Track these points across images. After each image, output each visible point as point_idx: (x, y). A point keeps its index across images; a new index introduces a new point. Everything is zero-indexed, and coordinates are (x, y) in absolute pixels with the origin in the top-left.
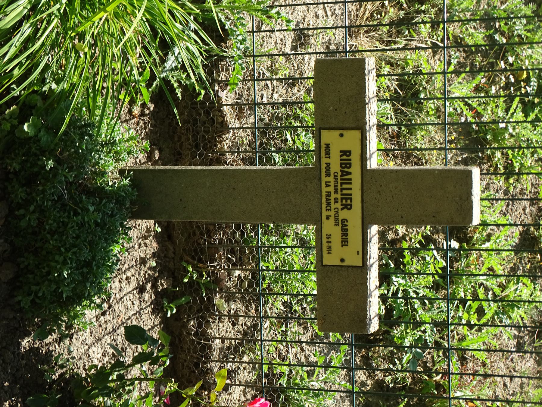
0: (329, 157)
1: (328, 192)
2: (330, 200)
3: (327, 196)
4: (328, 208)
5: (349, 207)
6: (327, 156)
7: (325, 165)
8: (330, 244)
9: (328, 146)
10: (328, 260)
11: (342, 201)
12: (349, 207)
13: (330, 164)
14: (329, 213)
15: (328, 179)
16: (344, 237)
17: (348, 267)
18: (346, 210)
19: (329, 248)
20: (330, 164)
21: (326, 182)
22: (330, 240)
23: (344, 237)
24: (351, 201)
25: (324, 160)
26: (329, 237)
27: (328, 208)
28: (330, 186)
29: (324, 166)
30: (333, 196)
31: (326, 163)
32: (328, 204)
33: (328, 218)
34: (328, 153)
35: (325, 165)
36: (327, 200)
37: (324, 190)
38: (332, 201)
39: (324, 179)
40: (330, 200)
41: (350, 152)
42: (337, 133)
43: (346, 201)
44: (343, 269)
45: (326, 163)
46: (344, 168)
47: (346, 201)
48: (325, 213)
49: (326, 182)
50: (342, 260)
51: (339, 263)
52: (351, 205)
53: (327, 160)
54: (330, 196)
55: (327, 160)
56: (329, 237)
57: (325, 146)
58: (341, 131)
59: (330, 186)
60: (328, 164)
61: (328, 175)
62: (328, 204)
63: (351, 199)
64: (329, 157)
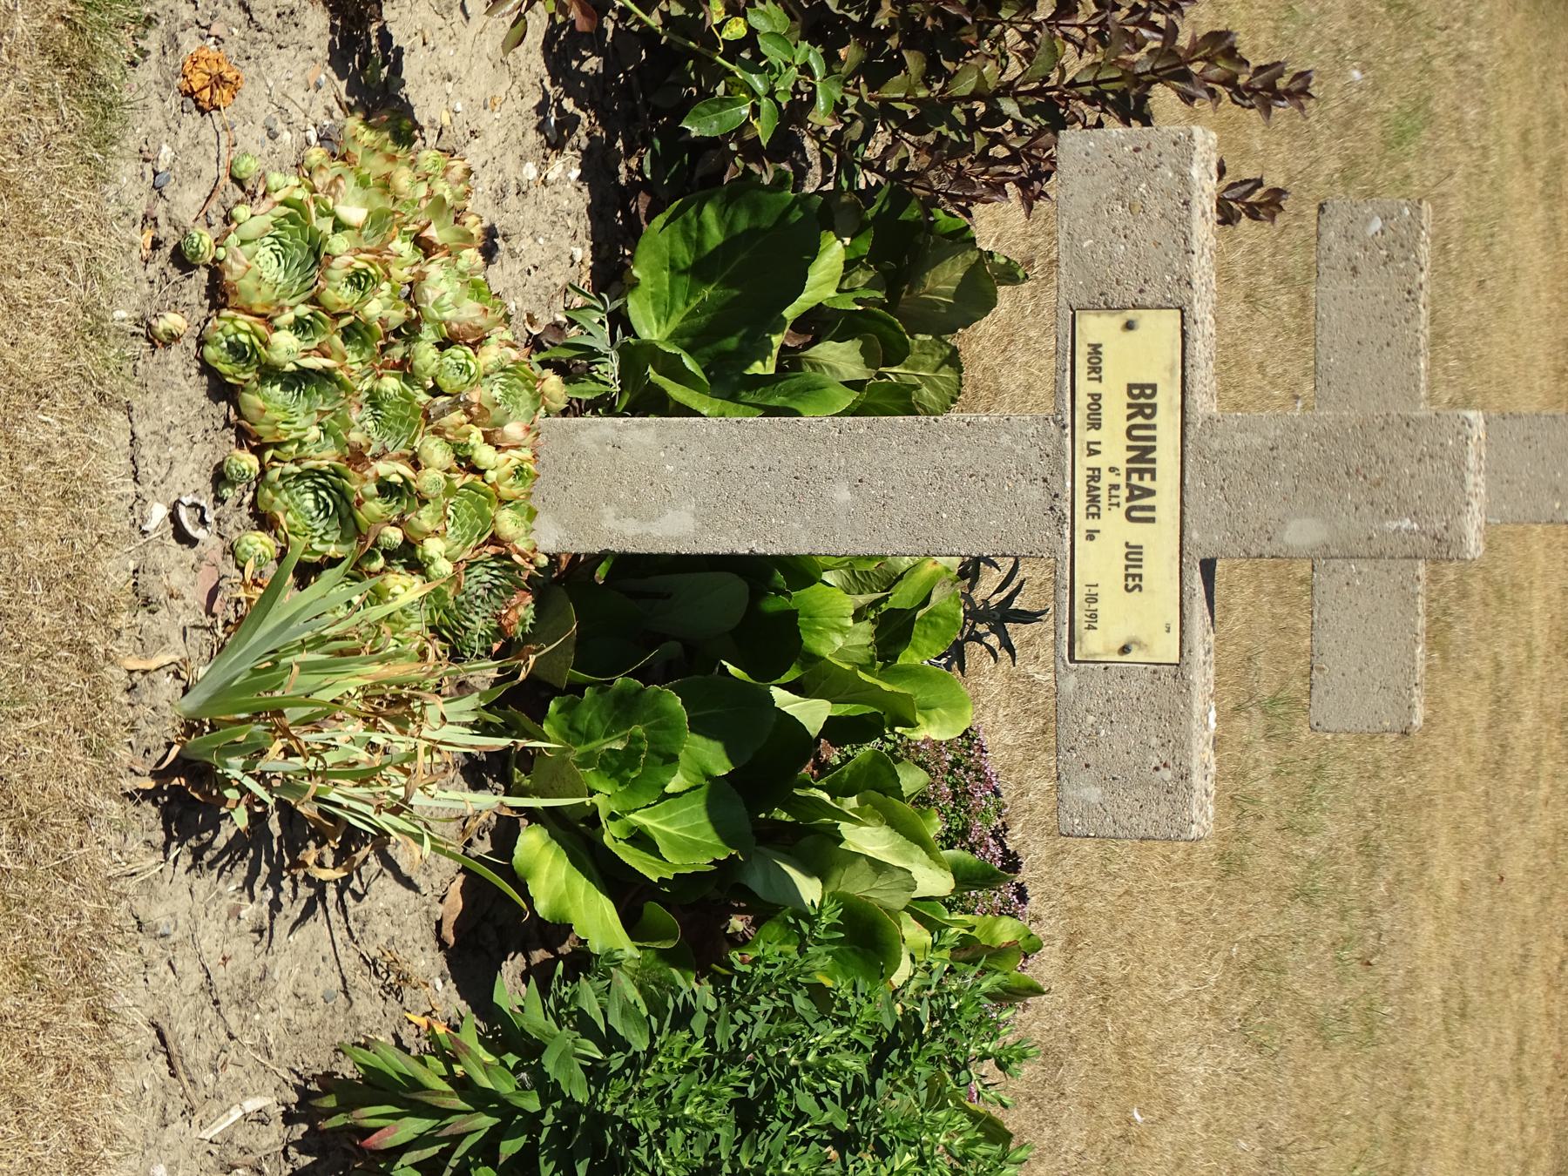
0: (1100, 379)
3: (1092, 478)
6: (1094, 375)
7: (1090, 400)
8: (1093, 606)
9: (1096, 349)
14: (1093, 524)
15: (1093, 435)
19: (1093, 616)
25: (1085, 386)
28: (1098, 452)
29: (1083, 401)
32: (1094, 500)
33: (1091, 536)
34: (1095, 368)
35: (1090, 400)
36: (1091, 489)
37: (1084, 462)
38: (1104, 494)
39: (1085, 435)
41: (1154, 387)
42: (1117, 321)
46: (1137, 397)
48: (1083, 524)
53: (1095, 387)
55: (1095, 387)
58: (1130, 314)
59: (1098, 452)
60: (1096, 398)
61: (1096, 425)
62: (1094, 500)
64: (1100, 379)
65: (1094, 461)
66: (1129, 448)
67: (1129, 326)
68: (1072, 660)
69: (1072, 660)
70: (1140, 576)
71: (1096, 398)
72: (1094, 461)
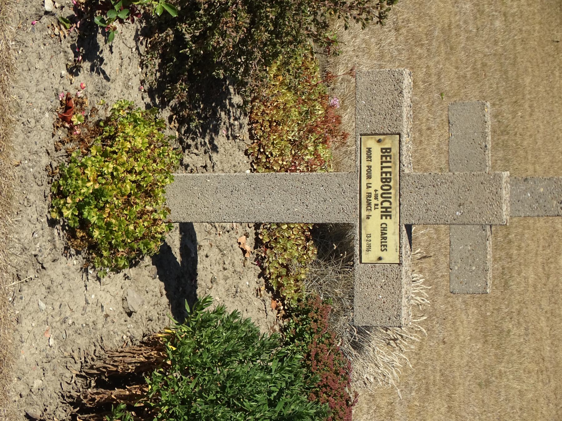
0: (371, 161)
4: (369, 208)
7: (367, 168)
8: (369, 243)
9: (369, 150)
19: (369, 246)
21: (367, 184)
26: (369, 236)
27: (369, 208)
28: (370, 187)
31: (368, 166)
32: (369, 204)
33: (368, 217)
34: (369, 157)
35: (367, 168)
45: (368, 166)
48: (364, 213)
50: (380, 259)
54: (370, 197)
58: (382, 137)
59: (370, 187)
60: (369, 167)
61: (369, 177)
62: (369, 204)
68: (361, 262)
69: (361, 262)
70: (386, 246)
71: (369, 167)
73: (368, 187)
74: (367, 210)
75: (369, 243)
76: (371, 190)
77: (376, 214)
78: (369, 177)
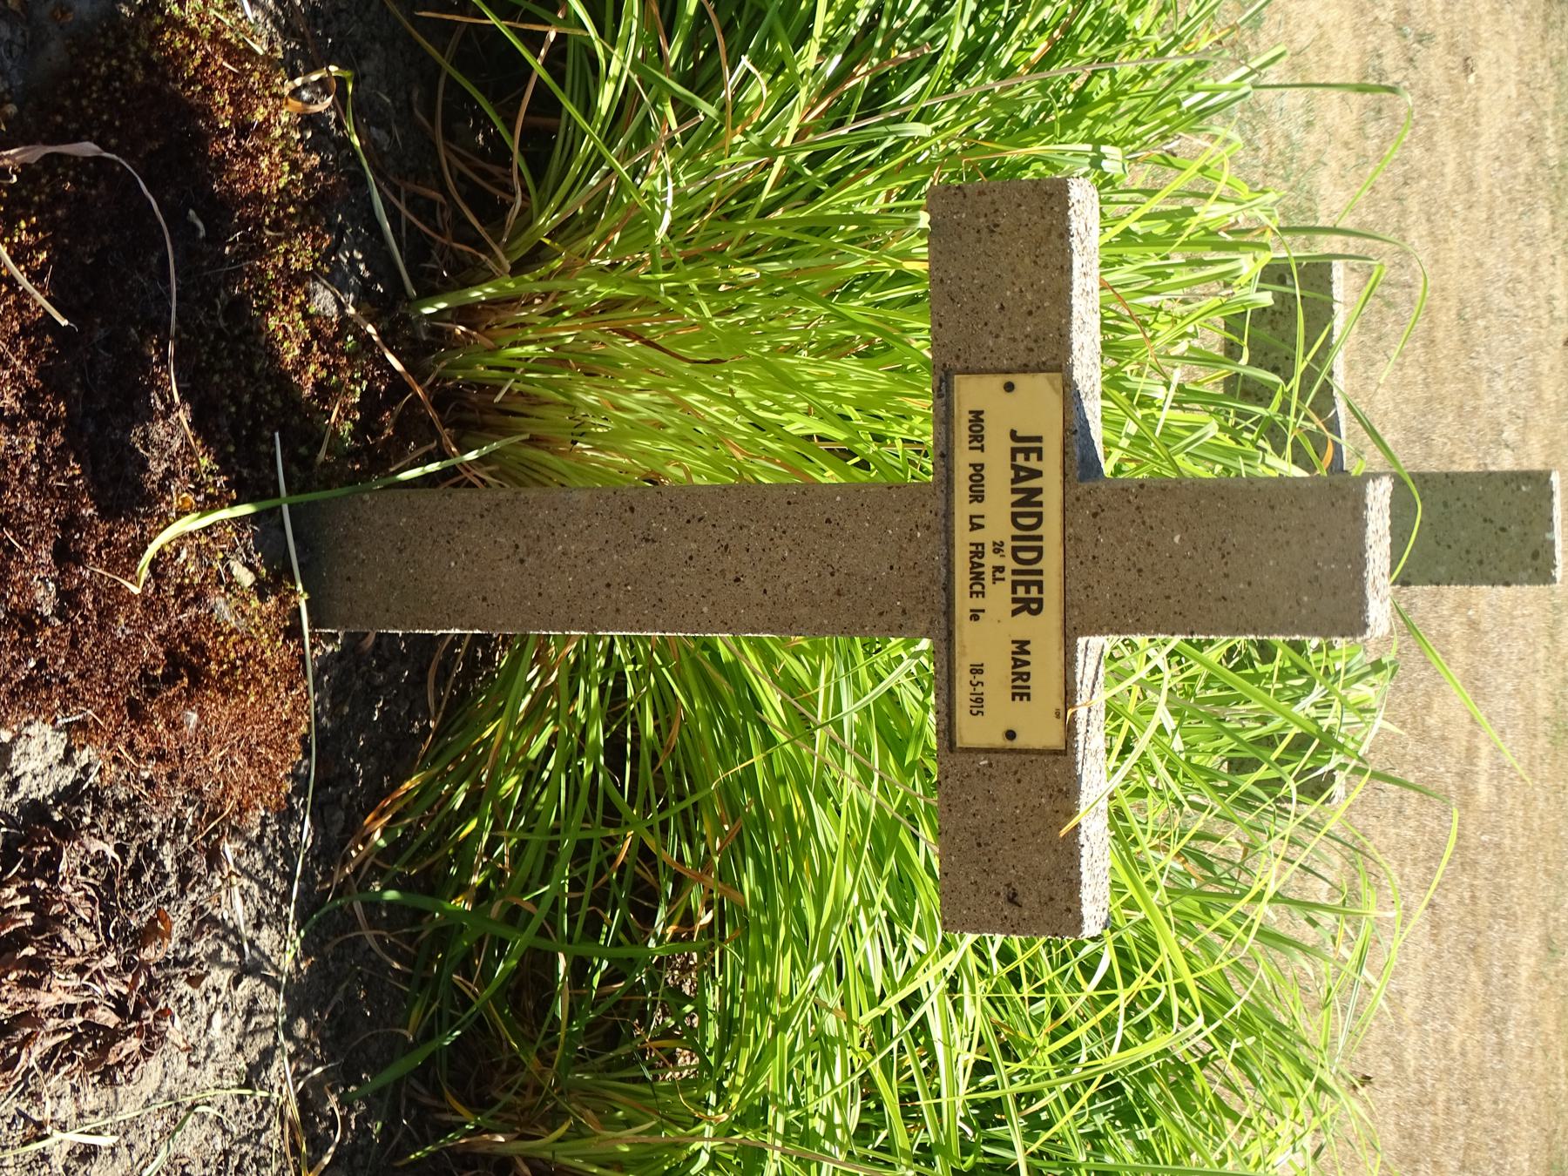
1: (977, 545)
2: (982, 565)
4: (977, 588)
5: (1034, 606)
6: (975, 444)
7: (971, 471)
8: (979, 689)
9: (977, 416)
10: (971, 732)
11: (1014, 591)
12: (1034, 606)
13: (982, 466)
14: (977, 603)
15: (976, 508)
16: (1019, 683)
17: (1027, 751)
18: (1025, 614)
19: (978, 700)
20: (982, 466)
21: (972, 517)
22: (979, 678)
23: (1019, 683)
24: (1040, 591)
26: (977, 670)
27: (977, 588)
28: (981, 527)
30: (990, 560)
31: (973, 465)
32: (977, 578)
33: (975, 616)
34: (977, 437)
36: (974, 565)
37: (963, 538)
39: (963, 508)
40: (982, 565)
43: (1028, 591)
44: (1011, 755)
45: (973, 465)
47: (1028, 591)
48: (963, 603)
49: (972, 517)
50: (1011, 735)
51: (999, 741)
52: (1040, 601)
53: (976, 457)
55: (976, 457)
56: (977, 670)
57: (971, 417)
59: (981, 527)
60: (978, 468)
61: (977, 496)
62: (977, 578)
63: (1040, 585)
65: (977, 536)
66: (1014, 491)
67: (1009, 387)
71: (978, 468)
72: (977, 536)
73: (975, 527)
74: (971, 594)
75: (979, 689)
76: (986, 537)
77: (999, 596)
78: (977, 496)
